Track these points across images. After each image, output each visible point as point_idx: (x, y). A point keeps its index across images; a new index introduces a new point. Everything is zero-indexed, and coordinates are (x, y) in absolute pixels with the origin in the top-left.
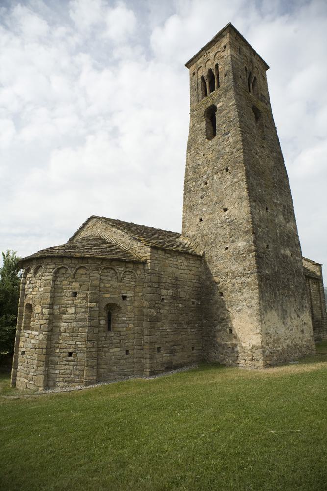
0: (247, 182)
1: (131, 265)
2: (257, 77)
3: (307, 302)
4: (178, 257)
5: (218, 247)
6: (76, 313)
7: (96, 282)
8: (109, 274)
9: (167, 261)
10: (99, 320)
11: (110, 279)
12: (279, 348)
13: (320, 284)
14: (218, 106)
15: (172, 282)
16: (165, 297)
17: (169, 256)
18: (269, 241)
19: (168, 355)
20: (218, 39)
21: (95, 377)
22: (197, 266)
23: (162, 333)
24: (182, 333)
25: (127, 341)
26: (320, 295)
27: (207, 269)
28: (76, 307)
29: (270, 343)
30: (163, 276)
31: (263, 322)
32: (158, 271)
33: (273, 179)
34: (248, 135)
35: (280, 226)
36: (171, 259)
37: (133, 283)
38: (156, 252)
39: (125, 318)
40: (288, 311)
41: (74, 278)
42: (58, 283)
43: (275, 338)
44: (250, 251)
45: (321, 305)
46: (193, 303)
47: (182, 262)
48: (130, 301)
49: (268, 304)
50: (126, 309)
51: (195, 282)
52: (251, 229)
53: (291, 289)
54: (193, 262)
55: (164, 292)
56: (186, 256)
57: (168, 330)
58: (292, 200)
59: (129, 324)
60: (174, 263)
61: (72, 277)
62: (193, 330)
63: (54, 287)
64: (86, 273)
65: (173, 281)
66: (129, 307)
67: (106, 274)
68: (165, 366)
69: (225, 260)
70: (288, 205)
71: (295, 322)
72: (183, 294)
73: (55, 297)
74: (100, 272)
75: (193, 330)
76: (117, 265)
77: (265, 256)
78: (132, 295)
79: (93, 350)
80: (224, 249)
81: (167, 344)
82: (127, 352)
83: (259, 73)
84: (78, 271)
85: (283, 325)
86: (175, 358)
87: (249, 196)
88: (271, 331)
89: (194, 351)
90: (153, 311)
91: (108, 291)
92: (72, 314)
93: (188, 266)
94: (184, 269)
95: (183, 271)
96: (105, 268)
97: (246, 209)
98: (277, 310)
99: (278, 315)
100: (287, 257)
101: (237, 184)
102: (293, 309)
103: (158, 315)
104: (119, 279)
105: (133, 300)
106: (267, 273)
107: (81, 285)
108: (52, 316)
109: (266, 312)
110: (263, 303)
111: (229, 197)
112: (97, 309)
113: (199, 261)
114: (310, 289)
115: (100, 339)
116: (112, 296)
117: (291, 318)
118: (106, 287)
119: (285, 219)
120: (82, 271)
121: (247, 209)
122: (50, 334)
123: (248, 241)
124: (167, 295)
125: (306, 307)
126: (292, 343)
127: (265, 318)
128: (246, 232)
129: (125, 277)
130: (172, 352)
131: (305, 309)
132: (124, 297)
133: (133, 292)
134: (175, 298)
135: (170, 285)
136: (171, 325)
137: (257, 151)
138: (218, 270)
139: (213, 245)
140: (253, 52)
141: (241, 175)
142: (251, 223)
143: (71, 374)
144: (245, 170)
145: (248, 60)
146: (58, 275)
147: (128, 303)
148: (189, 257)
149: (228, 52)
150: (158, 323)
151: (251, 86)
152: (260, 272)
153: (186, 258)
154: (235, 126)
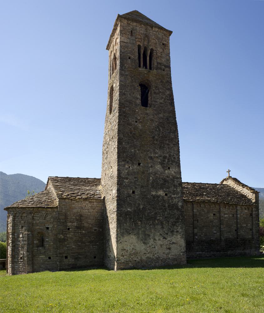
0: (118, 148)
1: (50, 210)
2: (154, 48)
3: (179, 228)
4: (83, 202)
6: (23, 237)
7: (30, 221)
8: (38, 216)
9: (73, 206)
10: (34, 241)
11: (39, 218)
12: (136, 259)
13: (254, 209)
15: (76, 218)
16: (70, 227)
17: (74, 202)
18: (136, 188)
19: (74, 260)
20: (116, 27)
21: (31, 270)
22: (100, 206)
23: (68, 248)
24: (85, 248)
25: (49, 252)
26: (252, 219)
28: (23, 234)
29: (126, 255)
30: (69, 215)
31: (119, 242)
32: (65, 212)
33: (153, 137)
34: (128, 108)
35: (156, 174)
36: (77, 204)
37: (52, 220)
38: (63, 201)
39: (48, 240)
40: (152, 235)
41: (21, 219)
42: (16, 221)
43: (133, 252)
45: (252, 226)
46: (95, 230)
47: (87, 205)
48: (51, 230)
49: (126, 231)
50: (49, 234)
51: (98, 217)
53: (158, 220)
55: (69, 224)
56: (90, 200)
57: (73, 246)
58: (179, 149)
59: (50, 243)
60: (79, 206)
61: (20, 218)
62: (94, 247)
63: (14, 224)
64: (26, 216)
65: (77, 217)
66: (50, 234)
67: (37, 216)
68: (71, 266)
70: (170, 155)
71: (159, 243)
72: (86, 225)
73: (15, 229)
74: (32, 215)
75: (94, 247)
76: (41, 210)
77: (129, 199)
78: (52, 227)
79: (30, 256)
81: (73, 254)
82: (50, 258)
83: (156, 43)
84: (23, 215)
85: (143, 244)
86: (79, 262)
87: (118, 158)
88: (129, 248)
89: (96, 259)
90: (61, 235)
91: (38, 225)
92: (21, 238)
93: (93, 207)
94: (88, 209)
95: (86, 210)
96: (35, 212)
98: (138, 234)
99: (138, 238)
100: (158, 197)
102: (159, 234)
103: (65, 238)
104: (44, 219)
105: (52, 229)
106: (128, 211)
107: (24, 222)
108: (14, 239)
109: (123, 236)
110: (120, 230)
112: (31, 235)
114: (237, 215)
115: (34, 251)
116: (40, 228)
117: (155, 239)
118: (37, 223)
119: (163, 167)
120: (25, 215)
121: (117, 167)
122: (14, 248)
124: (72, 226)
125: (177, 232)
126: (153, 256)
127: (122, 239)
129: (47, 217)
130: (76, 259)
131: (175, 233)
132: (48, 228)
133: (52, 225)
134: (79, 228)
135: (75, 220)
136: (76, 244)
137: (136, 118)
140: (148, 27)
143: (22, 268)
145: (142, 38)
146: (16, 217)
147: (49, 232)
148: (92, 201)
149: (118, 41)
150: (65, 242)
151: (148, 58)
152: (119, 210)
153: (90, 202)
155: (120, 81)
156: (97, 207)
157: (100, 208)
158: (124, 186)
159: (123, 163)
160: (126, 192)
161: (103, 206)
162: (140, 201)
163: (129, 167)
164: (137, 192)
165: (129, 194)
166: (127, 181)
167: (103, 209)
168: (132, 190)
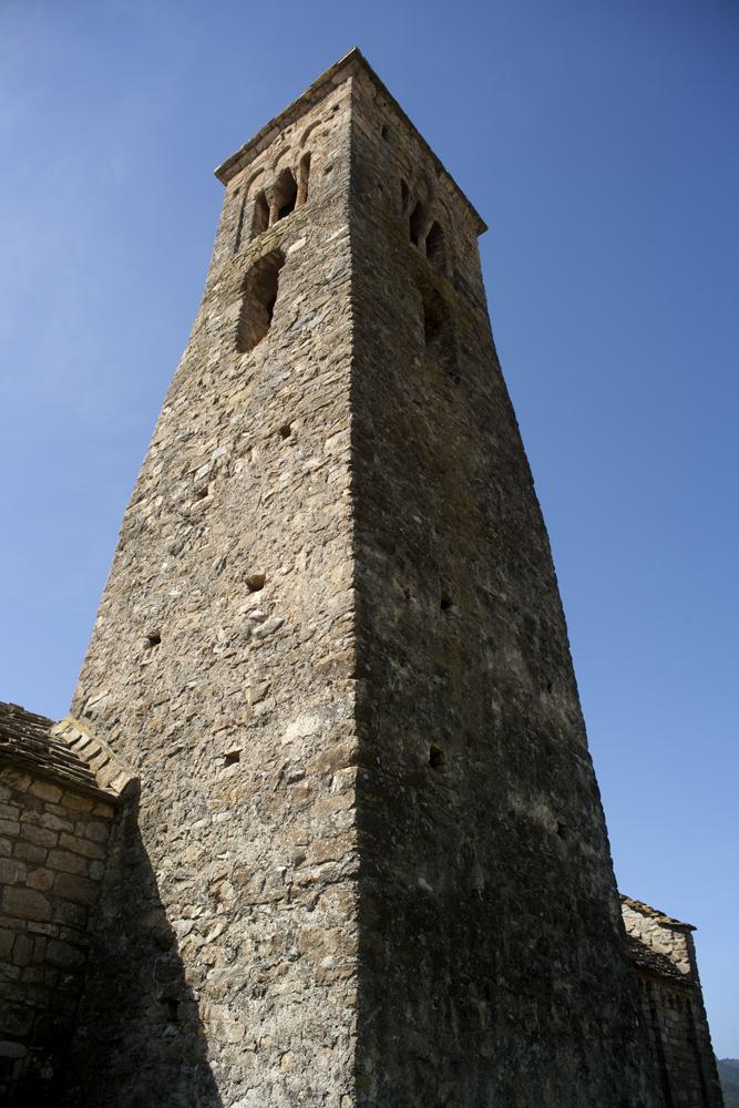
0: (354, 466)
5: (197, 752)
14: (291, 250)
22: (85, 848)
27: (133, 866)
44: (336, 763)
52: (351, 651)
54: (59, 824)
56: (24, 784)
69: (220, 817)
80: (222, 761)
87: (354, 515)
97: (340, 571)
101: (314, 477)
111: (275, 532)
113: (101, 826)
123: (334, 714)
128: (327, 669)
138: (177, 872)
139: (180, 743)
141: (338, 443)
142: (350, 625)
144: (353, 424)
148: (38, 790)
154: (335, 293)
155: (352, 226)
156: (58, 847)
157: (80, 865)
158: (391, 696)
159: (378, 555)
160: (401, 743)
161: (100, 854)
162: (472, 836)
163: (408, 597)
164: (454, 771)
165: (415, 760)
166: (403, 671)
167: (96, 876)
168: (429, 745)
